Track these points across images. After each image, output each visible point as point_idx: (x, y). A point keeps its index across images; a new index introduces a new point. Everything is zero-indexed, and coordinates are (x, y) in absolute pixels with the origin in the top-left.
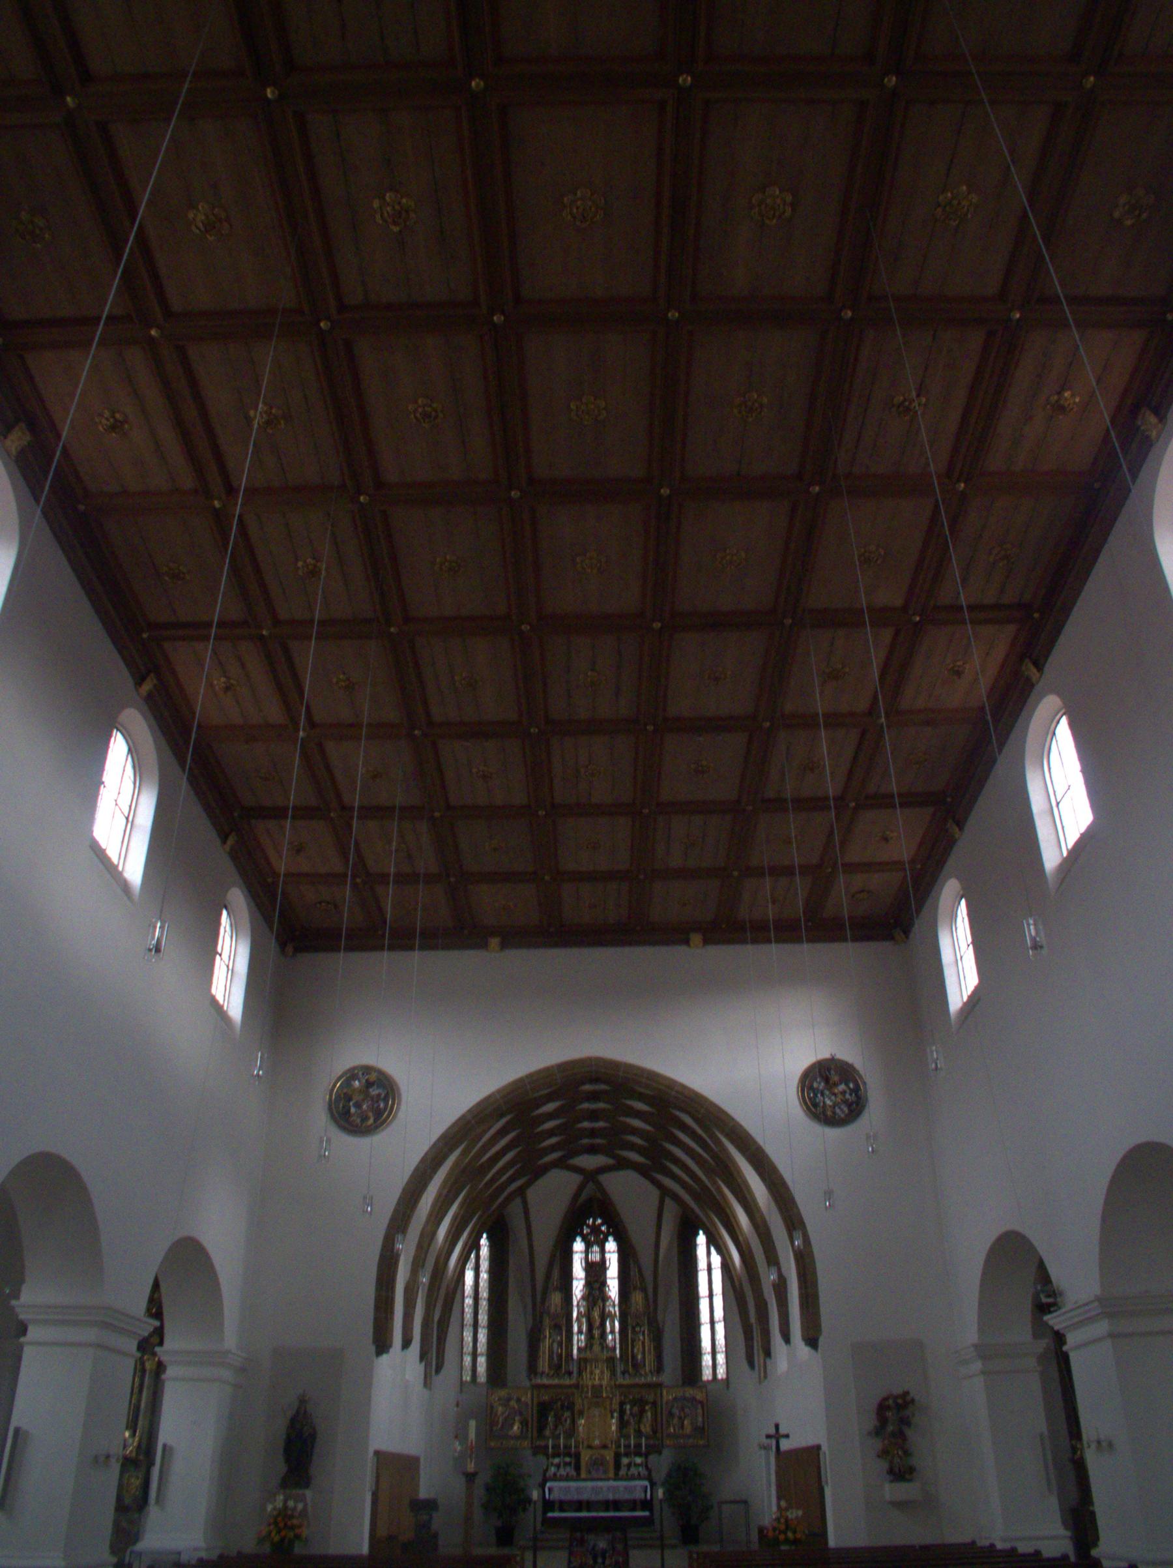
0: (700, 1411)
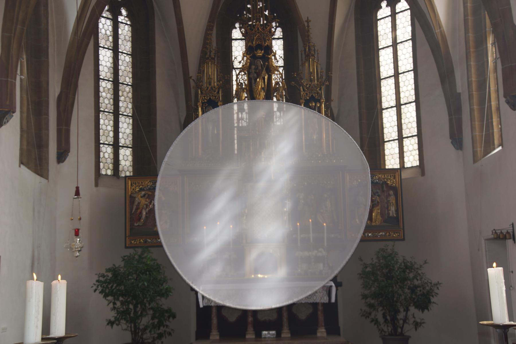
0: (392, 199)
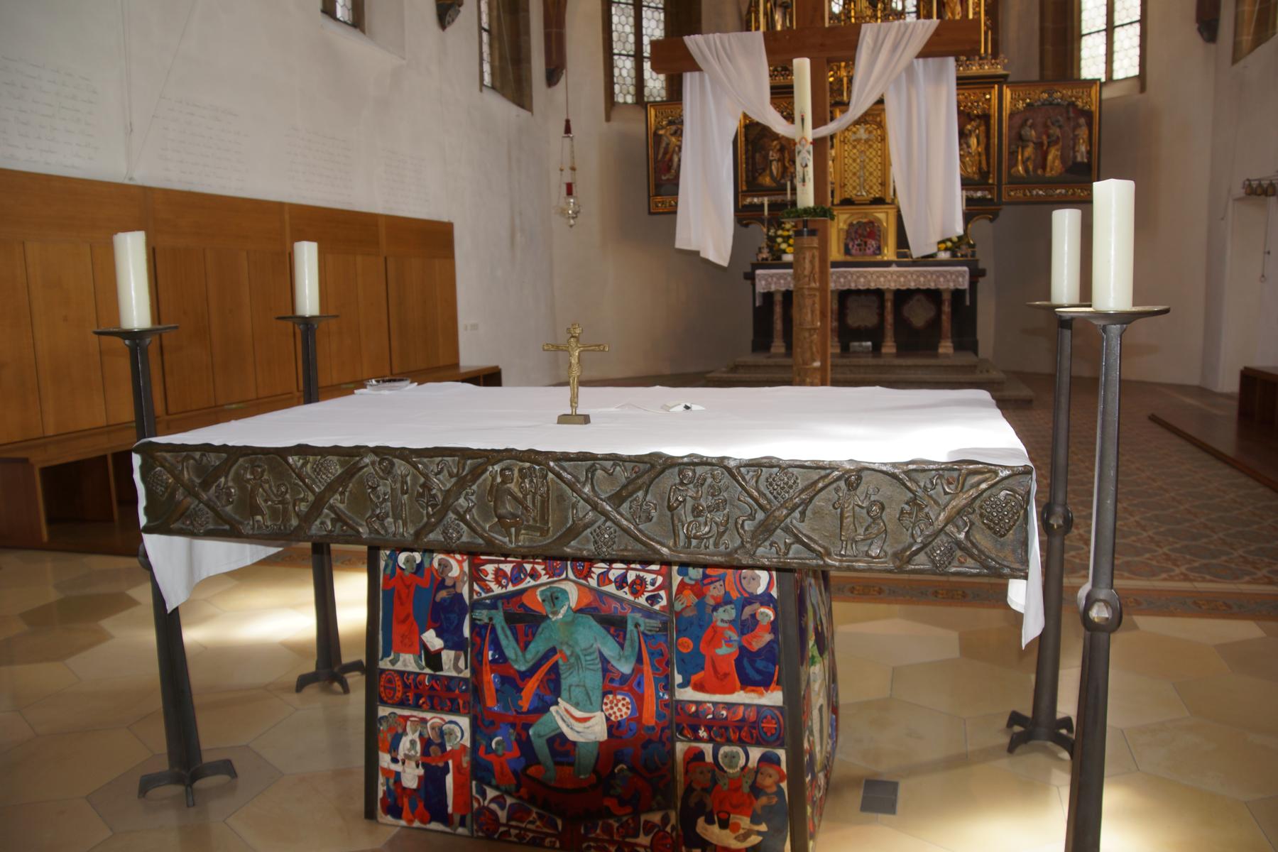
0: (1083, 132)
